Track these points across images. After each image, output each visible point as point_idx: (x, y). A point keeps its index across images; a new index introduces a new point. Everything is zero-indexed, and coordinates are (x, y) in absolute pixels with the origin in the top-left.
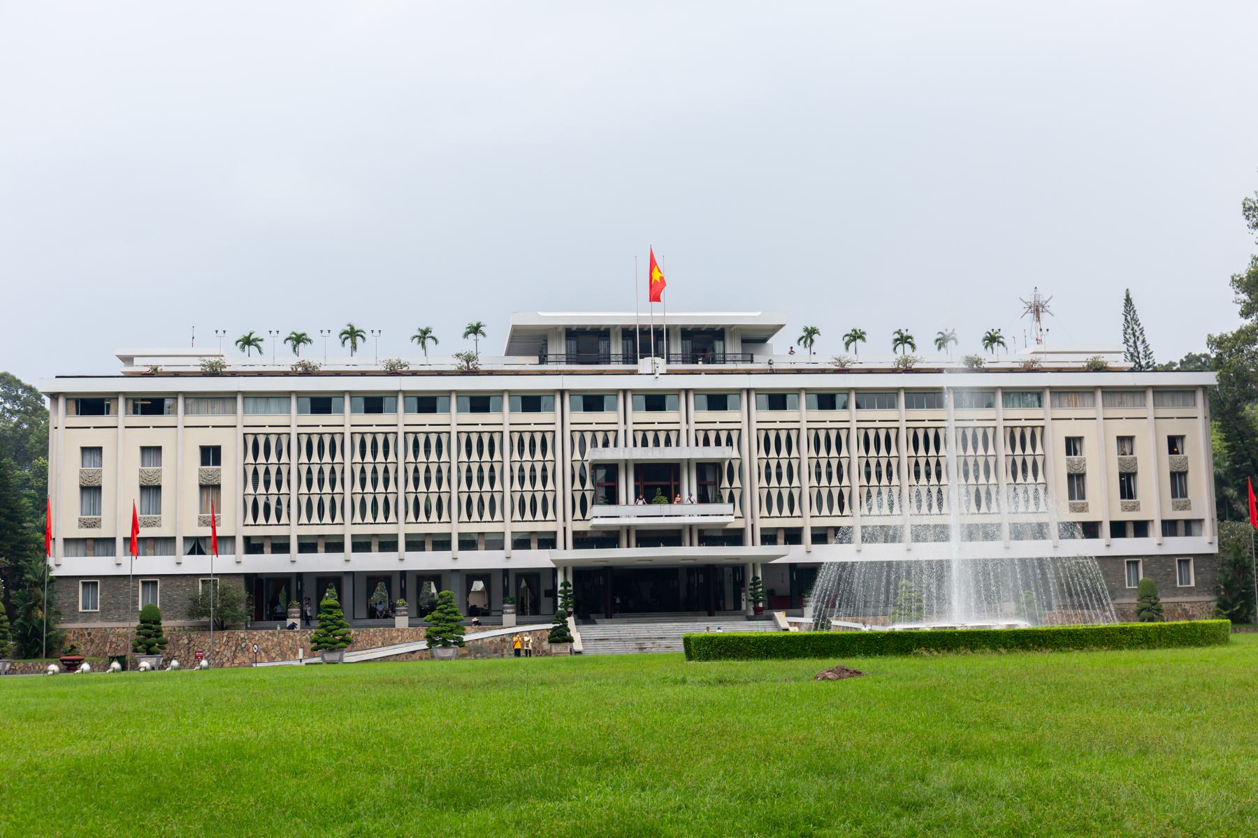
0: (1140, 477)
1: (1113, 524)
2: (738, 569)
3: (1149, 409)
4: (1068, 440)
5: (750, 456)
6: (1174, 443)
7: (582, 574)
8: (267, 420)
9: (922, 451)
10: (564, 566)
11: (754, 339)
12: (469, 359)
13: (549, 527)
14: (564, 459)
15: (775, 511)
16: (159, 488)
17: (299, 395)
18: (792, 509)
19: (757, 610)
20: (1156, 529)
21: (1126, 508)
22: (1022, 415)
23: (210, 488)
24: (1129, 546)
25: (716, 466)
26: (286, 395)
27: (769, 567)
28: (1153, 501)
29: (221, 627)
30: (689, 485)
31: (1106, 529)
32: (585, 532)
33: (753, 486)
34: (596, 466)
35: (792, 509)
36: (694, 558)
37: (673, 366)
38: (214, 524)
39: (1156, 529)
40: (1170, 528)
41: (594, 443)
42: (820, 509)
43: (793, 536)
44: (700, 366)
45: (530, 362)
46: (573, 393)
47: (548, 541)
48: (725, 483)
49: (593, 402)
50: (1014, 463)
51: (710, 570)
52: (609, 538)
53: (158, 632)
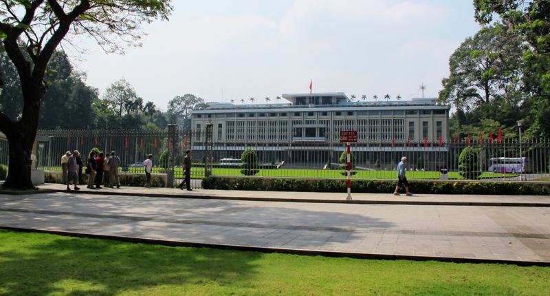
4: (410, 123)
8: (231, 119)
14: (289, 126)
23: (220, 133)
30: (317, 133)
33: (331, 133)
34: (297, 129)
40: (436, 145)
49: (297, 114)
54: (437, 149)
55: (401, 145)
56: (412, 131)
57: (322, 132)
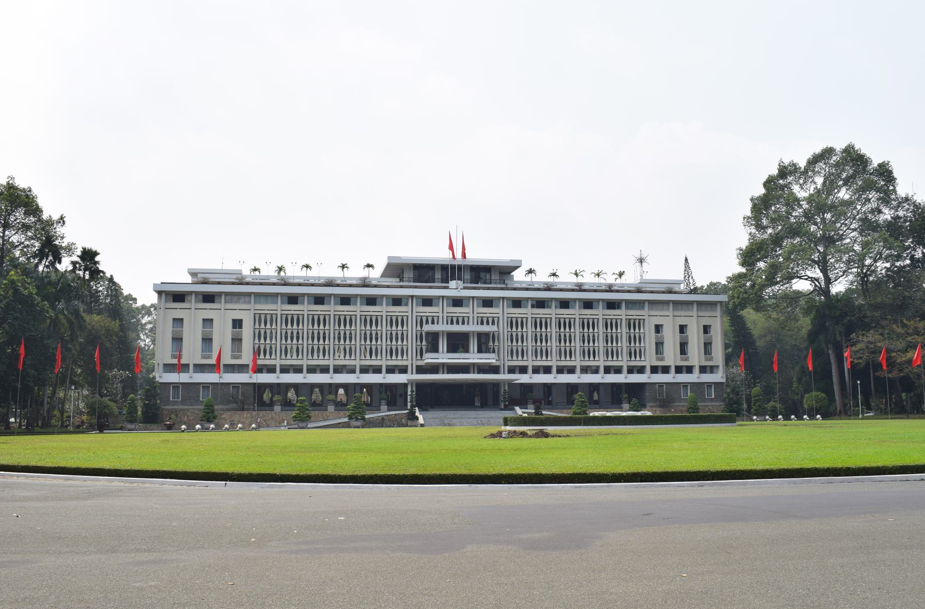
0: (689, 345)
1: (676, 367)
2: (496, 385)
3: (694, 313)
5: (502, 329)
6: (706, 329)
7: (420, 387)
9: (562, 329)
10: (411, 382)
11: (504, 272)
12: (365, 278)
13: (405, 363)
14: (411, 329)
15: (515, 358)
16: (211, 339)
17: (282, 295)
18: (523, 357)
19: (505, 406)
20: (697, 370)
21: (682, 360)
22: (634, 313)
23: (237, 341)
24: (683, 378)
25: (487, 335)
26: (275, 295)
27: (511, 384)
28: (695, 357)
29: (243, 410)
30: (473, 345)
31: (673, 369)
32: (421, 366)
33: (504, 345)
34: (428, 334)
35: (523, 357)
36: (476, 380)
37: (466, 285)
38: (179, 358)
39: (697, 370)
40: (703, 369)
41: (427, 322)
42: (536, 357)
43: (523, 370)
44: (479, 285)
45: (394, 281)
46: (417, 297)
47: (403, 370)
48: (491, 343)
49: (427, 302)
50: (630, 337)
51: (482, 385)
52: (434, 369)
53: (213, 411)
54: (707, 378)
55: (641, 370)
56: (659, 345)
57: (485, 342)
